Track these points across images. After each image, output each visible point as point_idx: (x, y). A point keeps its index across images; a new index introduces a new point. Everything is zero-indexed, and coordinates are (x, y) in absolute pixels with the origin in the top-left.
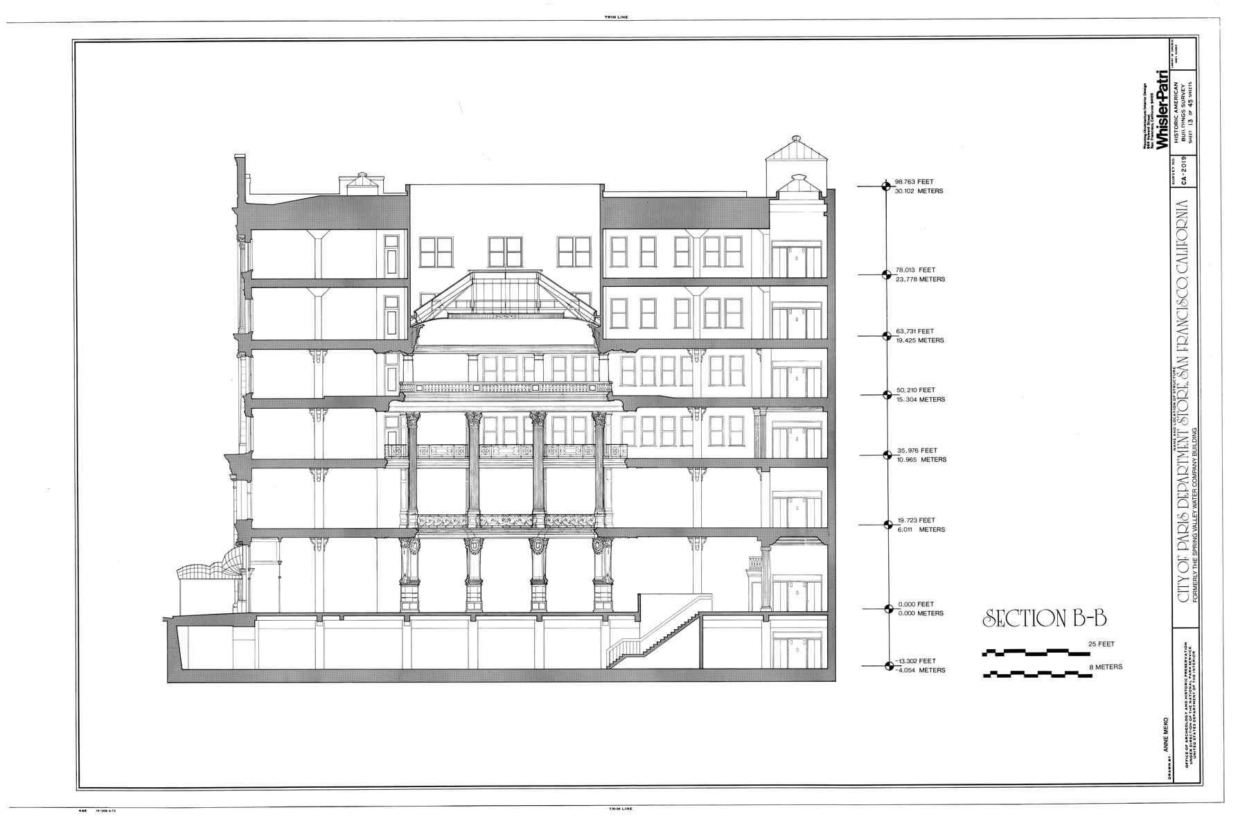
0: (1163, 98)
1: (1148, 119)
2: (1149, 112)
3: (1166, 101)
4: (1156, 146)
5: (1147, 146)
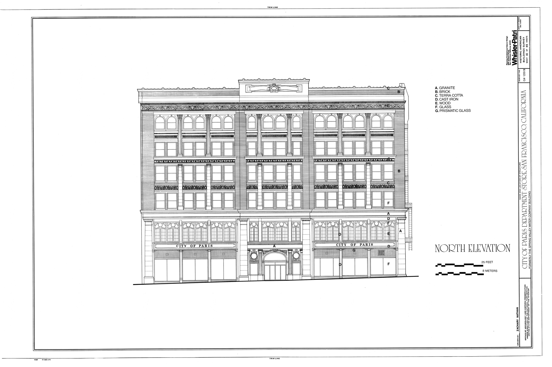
0: (515, 42)
1: (508, 52)
2: (509, 49)
3: (516, 44)
4: (512, 64)
5: (508, 64)
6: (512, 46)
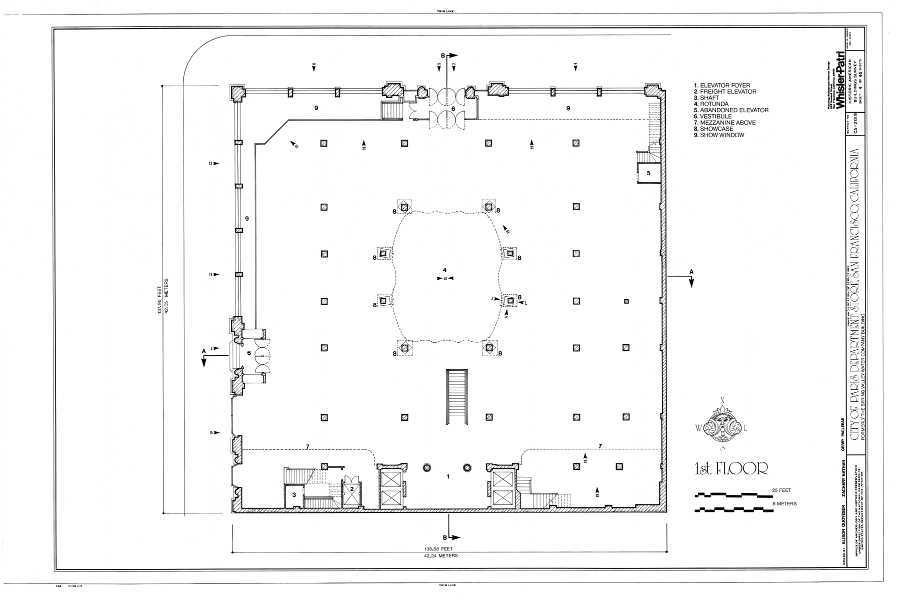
0: (841, 71)
1: (830, 87)
2: (832, 82)
3: (843, 74)
5: (830, 107)
6: (837, 78)
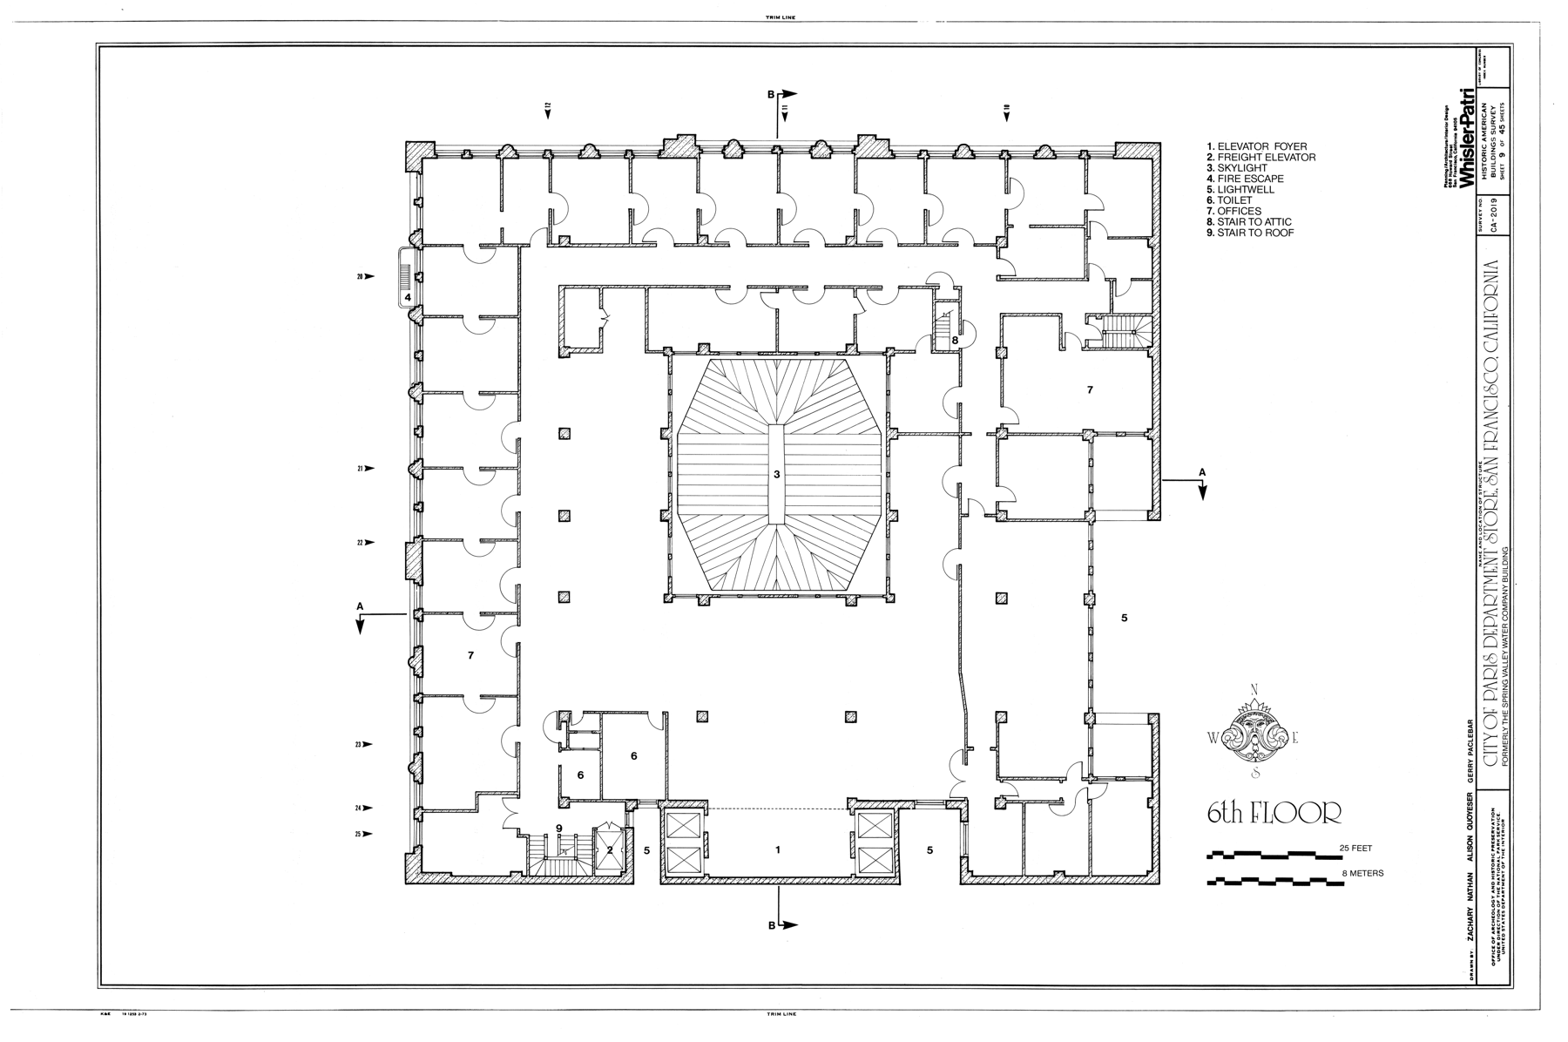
0: (1468, 123)
1: (1449, 151)
2: (1451, 142)
3: (1472, 127)
4: (1460, 183)
5: (1448, 184)
6: (1461, 134)
